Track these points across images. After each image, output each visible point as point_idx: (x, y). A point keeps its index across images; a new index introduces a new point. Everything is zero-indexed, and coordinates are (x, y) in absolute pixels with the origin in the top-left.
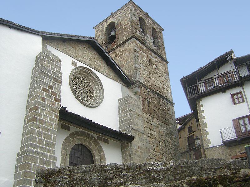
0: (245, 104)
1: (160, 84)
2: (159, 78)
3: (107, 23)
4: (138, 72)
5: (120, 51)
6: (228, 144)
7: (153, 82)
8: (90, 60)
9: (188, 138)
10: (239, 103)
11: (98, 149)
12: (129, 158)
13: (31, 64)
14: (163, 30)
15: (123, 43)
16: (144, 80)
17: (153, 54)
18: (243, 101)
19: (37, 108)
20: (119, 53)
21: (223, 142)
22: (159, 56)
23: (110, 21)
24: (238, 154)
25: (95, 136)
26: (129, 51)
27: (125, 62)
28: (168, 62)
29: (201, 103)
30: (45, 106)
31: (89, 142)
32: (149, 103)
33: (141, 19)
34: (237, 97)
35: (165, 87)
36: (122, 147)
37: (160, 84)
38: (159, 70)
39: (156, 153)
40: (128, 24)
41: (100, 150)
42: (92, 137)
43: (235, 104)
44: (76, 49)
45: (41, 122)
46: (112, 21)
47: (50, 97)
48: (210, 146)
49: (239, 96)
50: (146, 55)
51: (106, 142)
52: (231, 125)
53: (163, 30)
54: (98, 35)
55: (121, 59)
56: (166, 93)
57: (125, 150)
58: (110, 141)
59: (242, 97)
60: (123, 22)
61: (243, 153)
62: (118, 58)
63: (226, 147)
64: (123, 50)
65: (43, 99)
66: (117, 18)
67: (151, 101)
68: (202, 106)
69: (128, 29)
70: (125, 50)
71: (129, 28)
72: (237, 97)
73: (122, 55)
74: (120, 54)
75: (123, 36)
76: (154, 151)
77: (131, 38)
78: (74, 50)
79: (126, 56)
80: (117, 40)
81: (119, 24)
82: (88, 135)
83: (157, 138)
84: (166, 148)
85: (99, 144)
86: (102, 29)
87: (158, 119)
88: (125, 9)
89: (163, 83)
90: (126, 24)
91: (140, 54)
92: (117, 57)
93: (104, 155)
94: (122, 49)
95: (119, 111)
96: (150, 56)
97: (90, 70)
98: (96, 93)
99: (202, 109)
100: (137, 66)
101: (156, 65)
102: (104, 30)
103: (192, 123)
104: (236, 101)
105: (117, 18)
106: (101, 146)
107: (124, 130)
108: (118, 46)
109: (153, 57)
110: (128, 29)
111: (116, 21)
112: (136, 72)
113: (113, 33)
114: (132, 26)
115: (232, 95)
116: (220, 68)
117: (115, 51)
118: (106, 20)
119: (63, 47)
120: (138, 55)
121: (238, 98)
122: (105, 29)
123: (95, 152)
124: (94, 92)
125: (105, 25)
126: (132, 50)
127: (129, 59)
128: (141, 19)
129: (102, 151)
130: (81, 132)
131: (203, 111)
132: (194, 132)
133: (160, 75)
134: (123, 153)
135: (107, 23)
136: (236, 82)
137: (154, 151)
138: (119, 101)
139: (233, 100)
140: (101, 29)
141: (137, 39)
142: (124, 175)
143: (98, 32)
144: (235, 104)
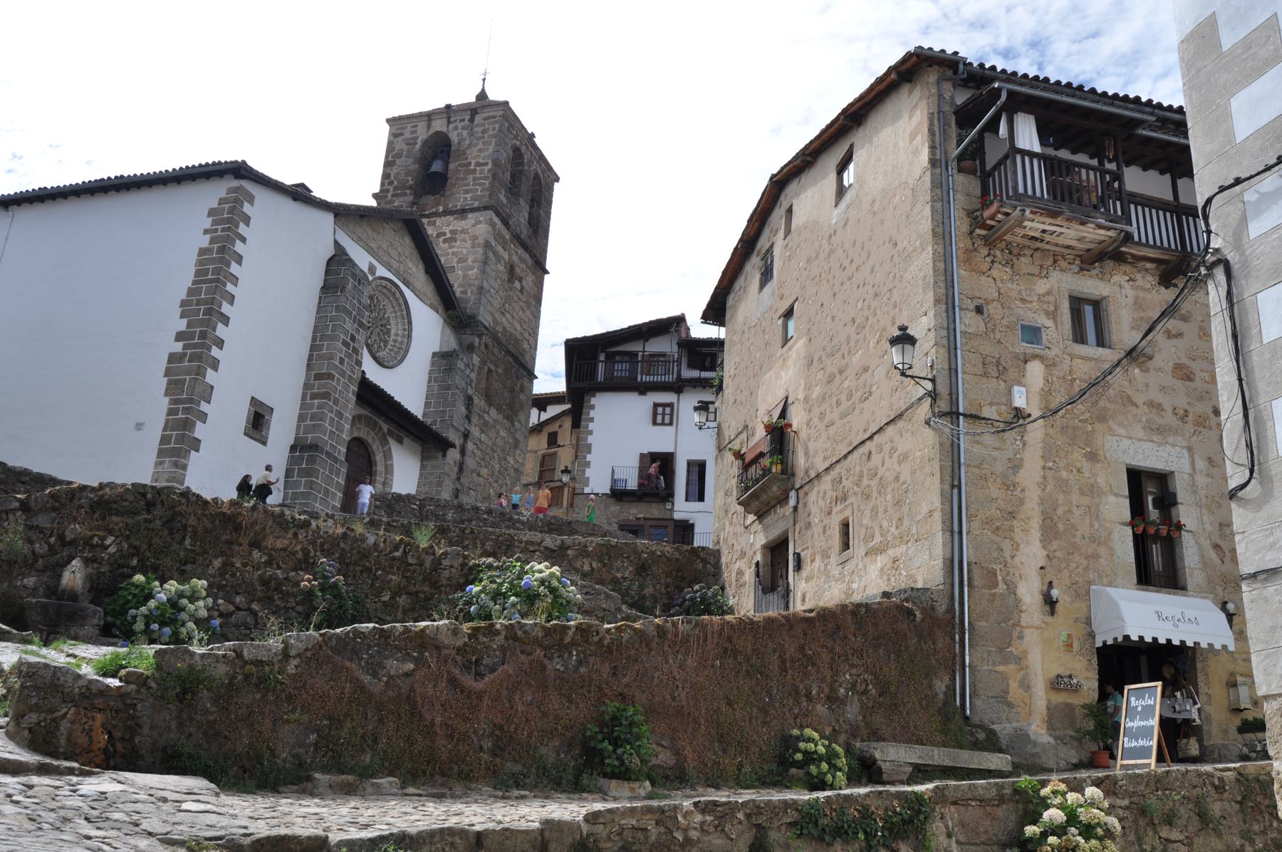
0: (671, 429)
1: (518, 328)
2: (521, 313)
3: (429, 127)
4: (484, 300)
5: (451, 228)
6: (619, 495)
7: (506, 324)
8: (400, 262)
9: (544, 457)
10: (663, 424)
11: (384, 452)
12: (434, 481)
13: (316, 279)
14: (557, 179)
15: (462, 213)
16: (490, 319)
17: (521, 251)
18: (671, 424)
19: (330, 376)
20: (446, 230)
21: (611, 490)
22: (533, 256)
23: (439, 125)
24: (631, 518)
25: (385, 427)
26: (475, 238)
27: (458, 263)
28: (547, 272)
29: (593, 401)
30: (343, 374)
31: (373, 438)
32: (490, 371)
33: (516, 150)
34: (664, 410)
35: (526, 335)
36: (422, 456)
37: (518, 328)
38: (525, 292)
39: (481, 479)
40: (483, 165)
41: (388, 456)
42: (381, 428)
43: (655, 423)
44: (379, 233)
45: (336, 402)
46: (444, 129)
47: (349, 356)
48: (587, 490)
49: (668, 410)
50: (506, 256)
51: (400, 441)
52: (635, 463)
53: (557, 179)
54: (397, 148)
55: (450, 251)
56: (524, 351)
57: (428, 463)
58: (406, 440)
59: (671, 415)
60: (474, 151)
61: (639, 519)
62: (442, 244)
63: (613, 500)
64: (459, 229)
65: (342, 361)
66: (459, 131)
67: (493, 368)
68: (593, 407)
69: (481, 178)
70: (464, 231)
71: (486, 178)
72: (664, 410)
73: (452, 240)
74: (449, 235)
75: (466, 192)
76: (479, 475)
77: (486, 208)
78: (375, 235)
79: (463, 247)
80: (448, 193)
81: (462, 153)
82: (376, 423)
83: (489, 451)
84: (499, 472)
85: (388, 443)
86: (412, 139)
87: (499, 409)
88: (486, 115)
89: (525, 326)
90: (481, 161)
91: (496, 254)
92: (441, 239)
93: (392, 465)
94: (459, 225)
95: (430, 381)
96: (515, 258)
97: (397, 286)
98: (397, 335)
99: (592, 414)
100: (486, 285)
101: (520, 280)
102: (418, 146)
103: (560, 426)
104: (659, 419)
105: (459, 131)
106: (390, 448)
107: (435, 422)
108: (447, 212)
109: (520, 258)
110: (481, 178)
111: (454, 137)
112: (480, 299)
113: (437, 166)
114: (495, 176)
115: (656, 405)
116: (651, 341)
117: (439, 221)
118: (429, 116)
119: (359, 230)
120: (491, 255)
121: (664, 414)
122: (419, 141)
123: (379, 457)
124: (393, 331)
125: (423, 134)
126: (481, 241)
127: (470, 260)
128: (516, 150)
129: (391, 458)
130: (366, 416)
131: (592, 420)
132: (559, 446)
133: (522, 303)
134: (423, 467)
135: (429, 127)
136: (669, 382)
137: (479, 475)
138: (433, 357)
139: (655, 414)
140: (407, 135)
141: (498, 214)
142: (485, 519)
143: (399, 139)
144: (655, 423)
